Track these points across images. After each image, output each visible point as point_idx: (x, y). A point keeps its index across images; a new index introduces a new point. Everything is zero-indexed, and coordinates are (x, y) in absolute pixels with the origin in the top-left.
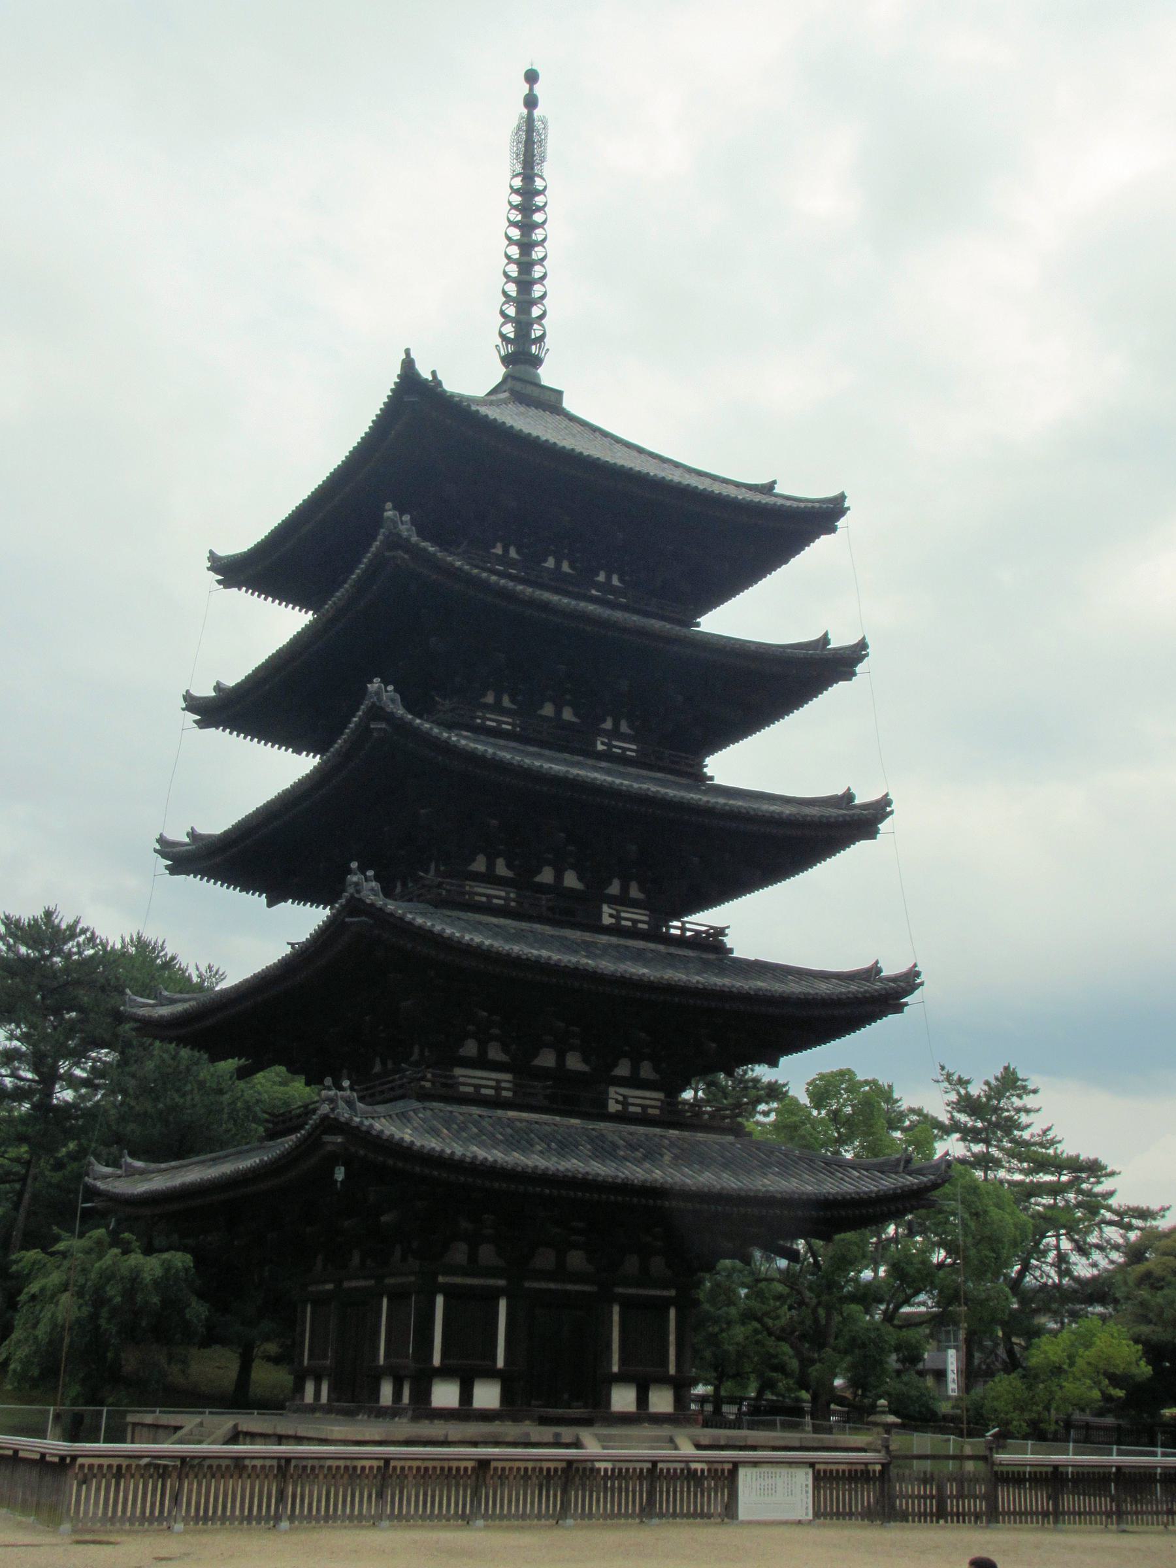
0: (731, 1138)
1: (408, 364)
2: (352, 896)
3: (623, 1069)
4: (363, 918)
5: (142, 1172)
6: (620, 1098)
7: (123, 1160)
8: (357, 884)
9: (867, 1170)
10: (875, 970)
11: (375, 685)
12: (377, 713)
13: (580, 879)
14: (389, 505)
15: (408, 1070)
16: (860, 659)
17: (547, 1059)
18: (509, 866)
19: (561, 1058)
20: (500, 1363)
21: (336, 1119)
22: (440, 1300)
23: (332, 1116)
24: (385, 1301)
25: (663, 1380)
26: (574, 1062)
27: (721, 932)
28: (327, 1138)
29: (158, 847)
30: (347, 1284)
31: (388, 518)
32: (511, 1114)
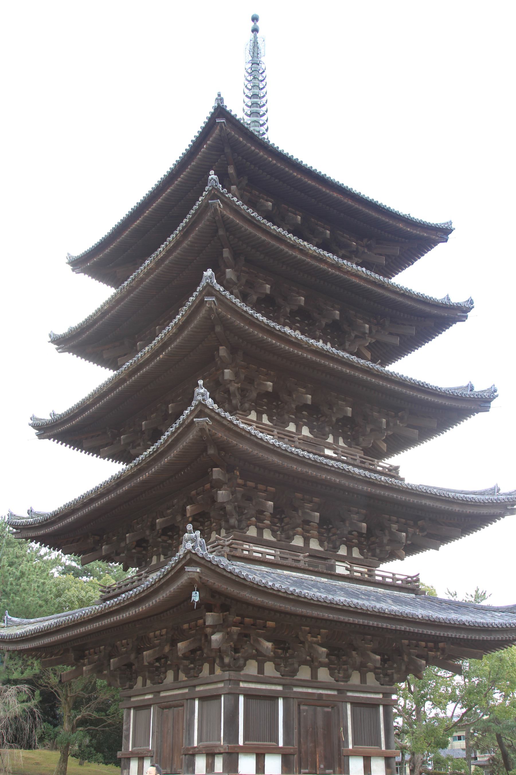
0: (413, 595)
1: (220, 99)
2: (200, 402)
3: (343, 551)
4: (207, 418)
5: (19, 624)
6: (349, 566)
7: (6, 617)
8: (203, 395)
9: (503, 612)
10: (495, 490)
11: (209, 272)
12: (209, 290)
13: (310, 432)
14: (212, 172)
15: (221, 540)
16: (469, 309)
17: (298, 542)
18: (270, 420)
19: (307, 541)
20: (281, 744)
21: (196, 554)
22: (241, 699)
23: (193, 552)
24: (197, 702)
25: (379, 755)
26: (314, 545)
27: (396, 469)
28: (187, 569)
29: (31, 422)
30: (162, 694)
31: (212, 178)
32: (286, 572)
